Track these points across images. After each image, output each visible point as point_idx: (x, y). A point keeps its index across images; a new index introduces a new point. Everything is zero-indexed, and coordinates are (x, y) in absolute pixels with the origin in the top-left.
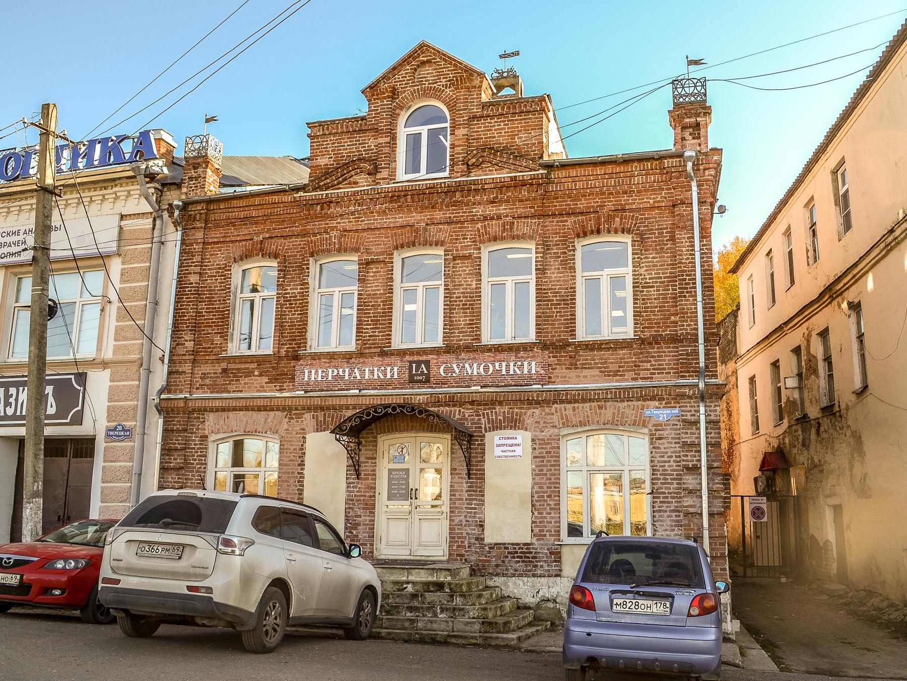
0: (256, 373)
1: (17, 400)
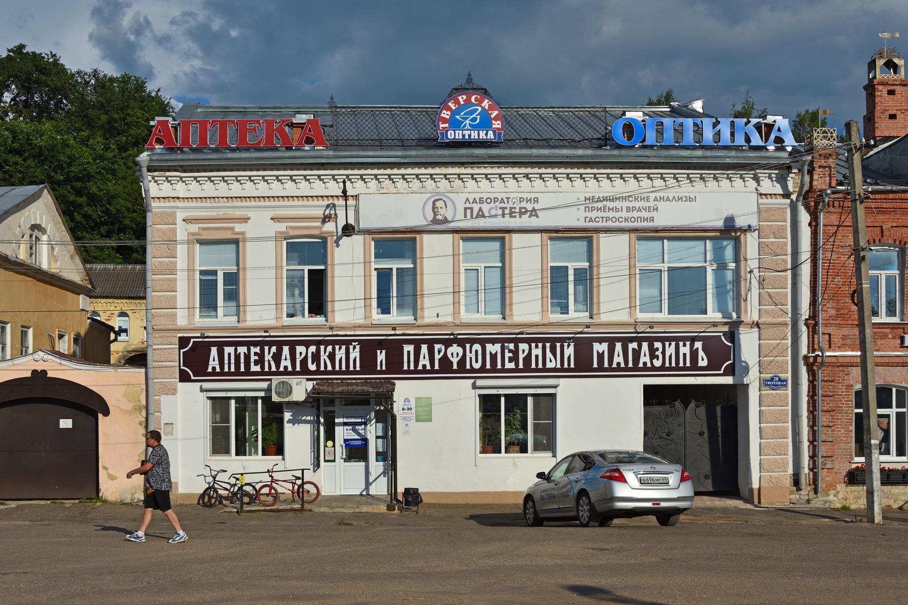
0: (890, 336)
1: (664, 353)
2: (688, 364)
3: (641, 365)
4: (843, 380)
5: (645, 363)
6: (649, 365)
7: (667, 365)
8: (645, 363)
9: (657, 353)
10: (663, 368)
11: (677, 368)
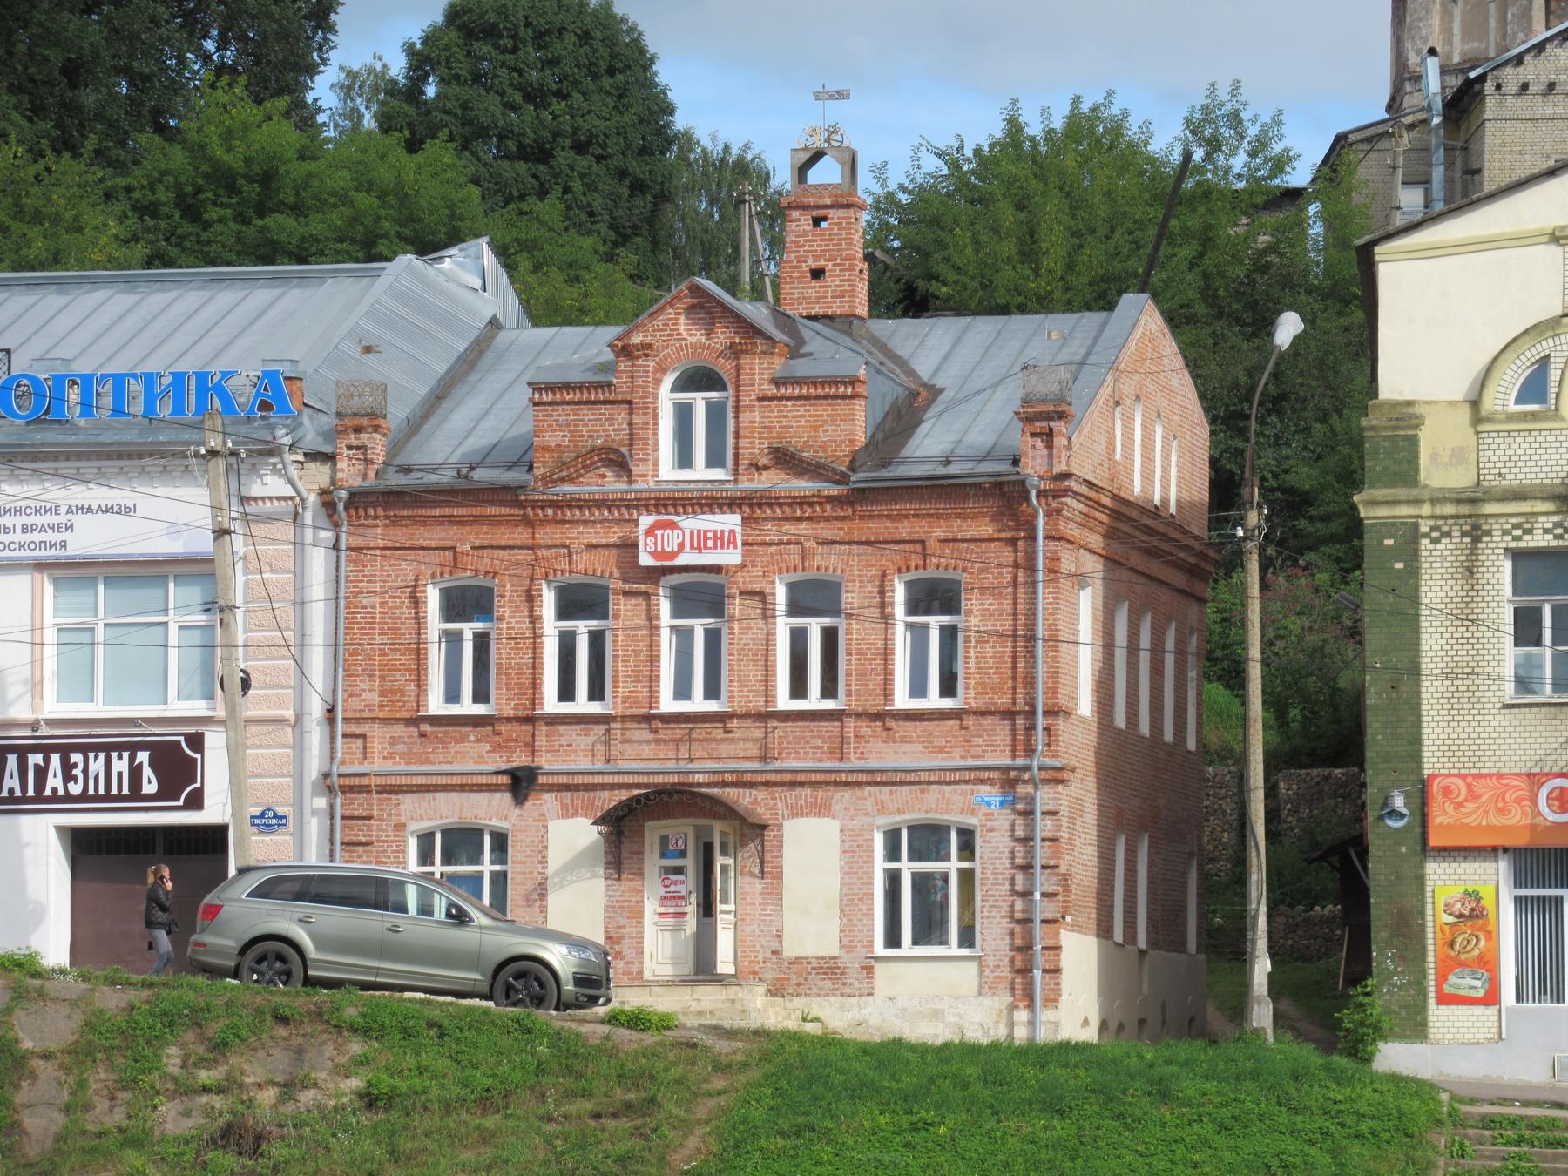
0: (472, 738)
1: (85, 771)
2: (125, 791)
3: (48, 792)
4: (390, 814)
5: (55, 790)
6: (61, 792)
7: (91, 792)
8: (55, 790)
9: (75, 772)
10: (84, 797)
11: (108, 797)
